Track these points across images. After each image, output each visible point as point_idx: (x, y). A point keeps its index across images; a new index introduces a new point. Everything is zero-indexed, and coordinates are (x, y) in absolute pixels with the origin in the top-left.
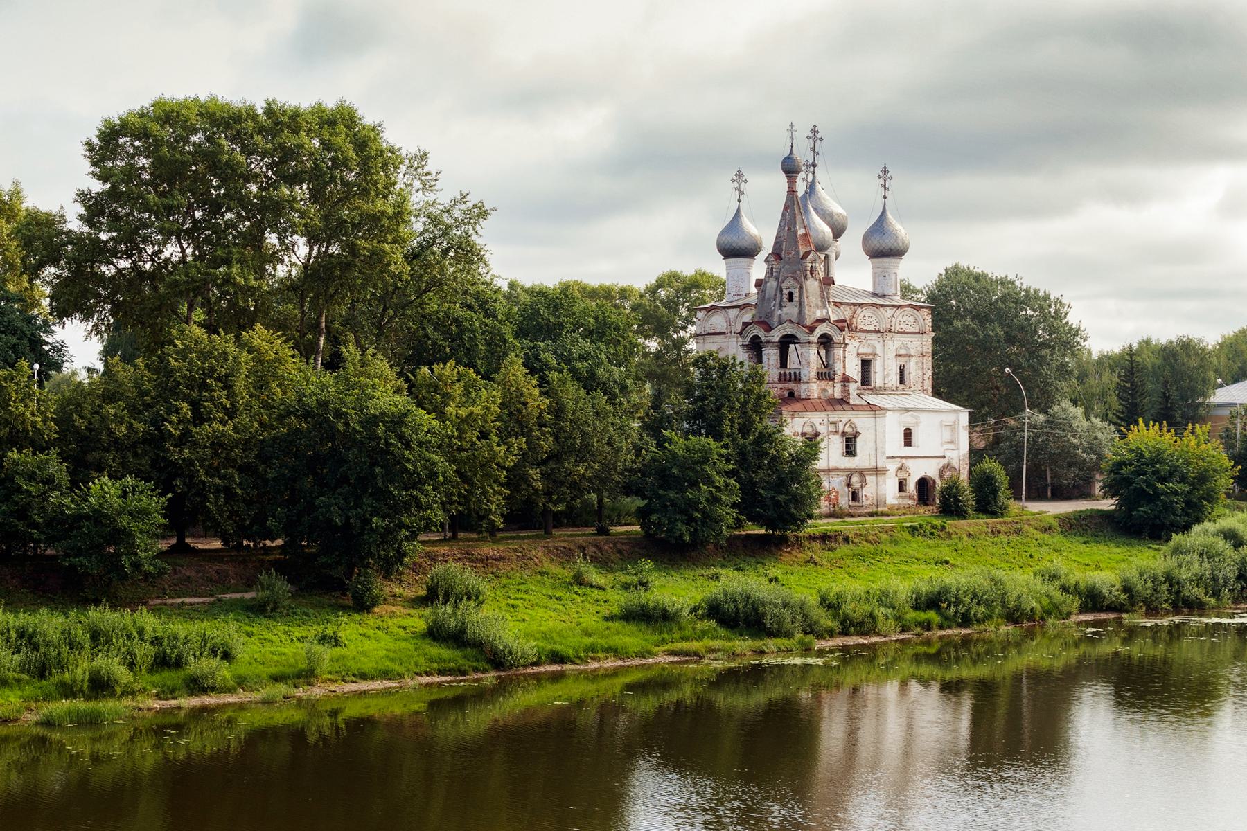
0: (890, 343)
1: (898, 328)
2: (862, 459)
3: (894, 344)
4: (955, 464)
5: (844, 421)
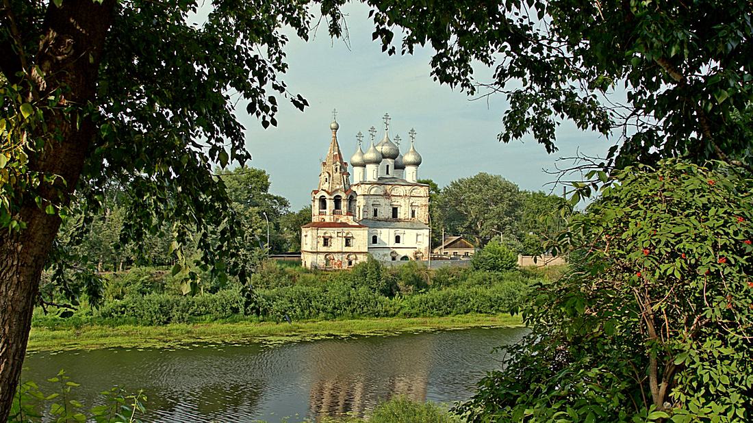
5: (346, 232)
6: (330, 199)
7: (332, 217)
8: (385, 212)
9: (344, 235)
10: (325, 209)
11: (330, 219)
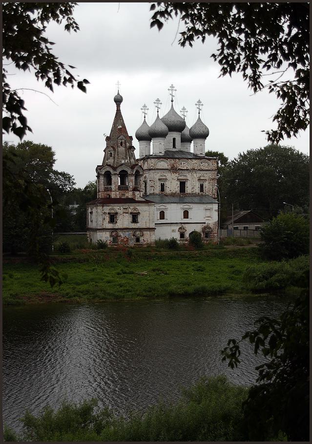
0: (195, 175)
1: (199, 168)
2: (142, 223)
3: (197, 175)
4: (211, 226)
6: (115, 174)
7: (118, 193)
8: (173, 186)
9: (130, 211)
10: (111, 184)
11: (116, 195)
